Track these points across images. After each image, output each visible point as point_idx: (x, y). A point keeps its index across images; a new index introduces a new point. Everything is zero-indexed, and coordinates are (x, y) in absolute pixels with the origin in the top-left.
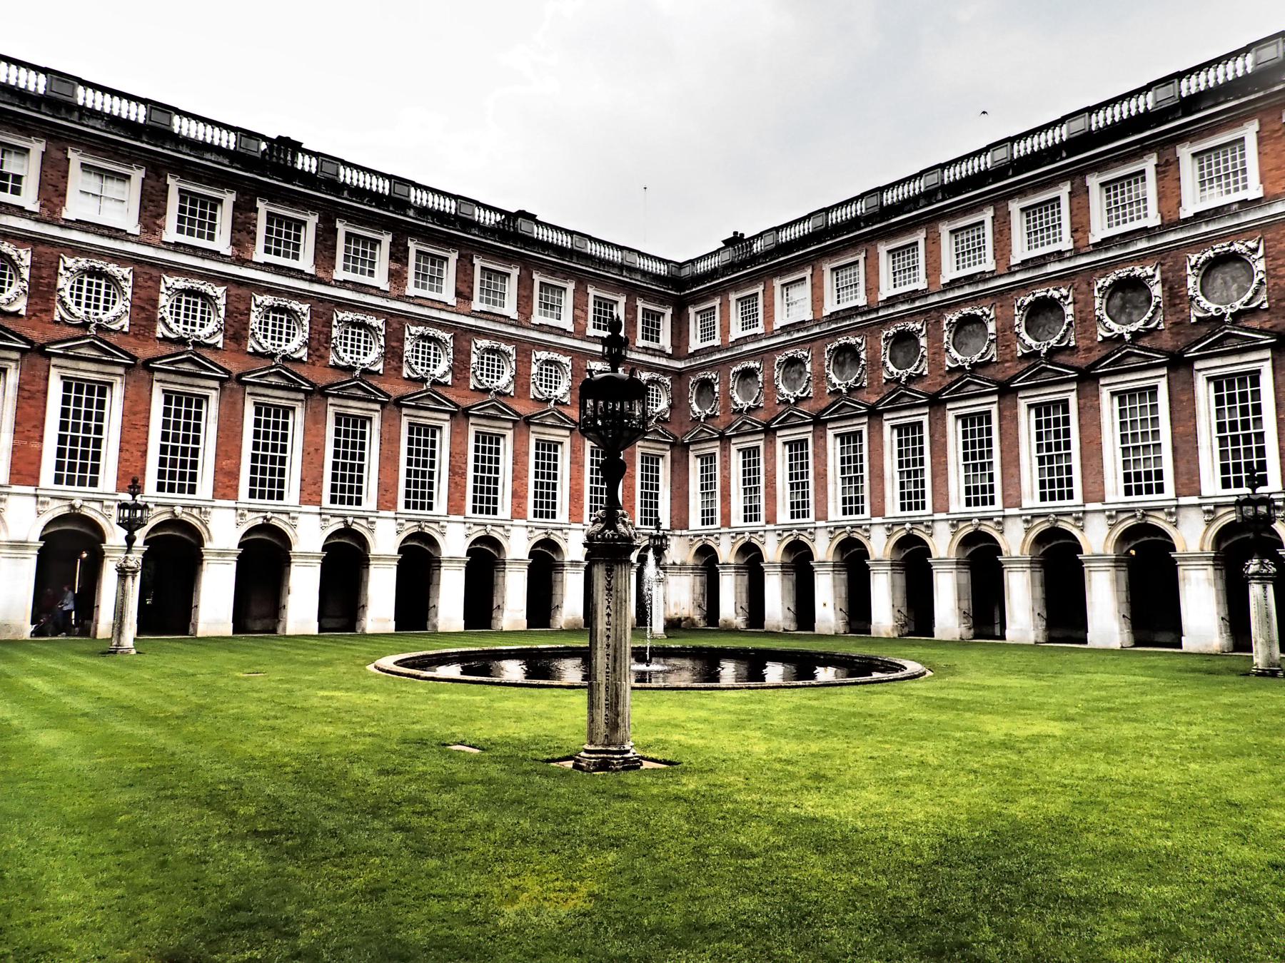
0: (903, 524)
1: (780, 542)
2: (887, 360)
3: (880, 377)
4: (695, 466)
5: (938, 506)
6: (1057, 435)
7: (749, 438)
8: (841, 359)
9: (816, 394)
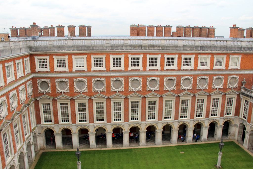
0: (117, 124)
1: (77, 128)
2: (112, 86)
3: (110, 90)
4: (41, 106)
5: (125, 120)
6: (153, 107)
7: (64, 101)
8: (97, 83)
9: (88, 92)
